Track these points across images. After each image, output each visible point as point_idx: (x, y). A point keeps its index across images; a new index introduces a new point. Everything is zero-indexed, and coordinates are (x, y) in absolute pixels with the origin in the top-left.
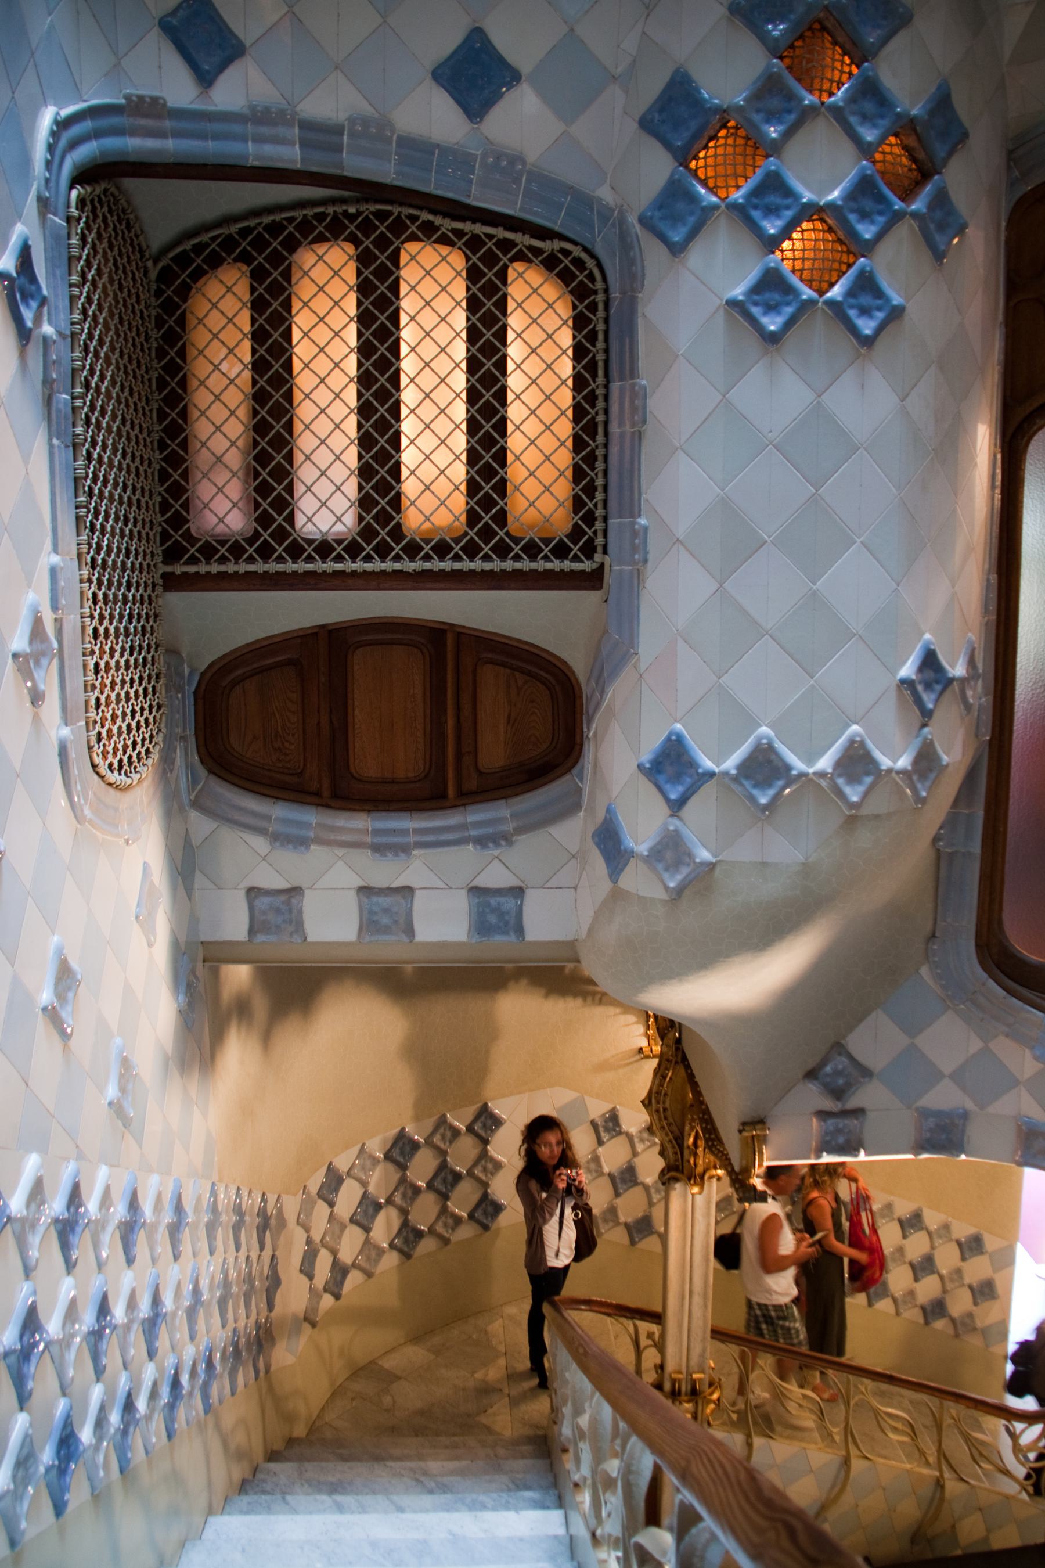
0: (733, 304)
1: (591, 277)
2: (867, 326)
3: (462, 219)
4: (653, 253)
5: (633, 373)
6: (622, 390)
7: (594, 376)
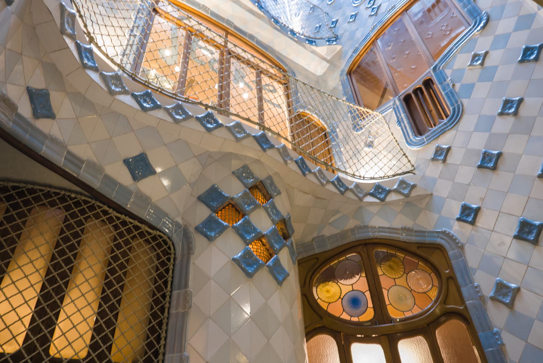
0: (234, 260)
1: (169, 248)
2: (281, 279)
3: (121, 213)
4: (199, 241)
5: (186, 286)
6: (179, 295)
7: (166, 287)
